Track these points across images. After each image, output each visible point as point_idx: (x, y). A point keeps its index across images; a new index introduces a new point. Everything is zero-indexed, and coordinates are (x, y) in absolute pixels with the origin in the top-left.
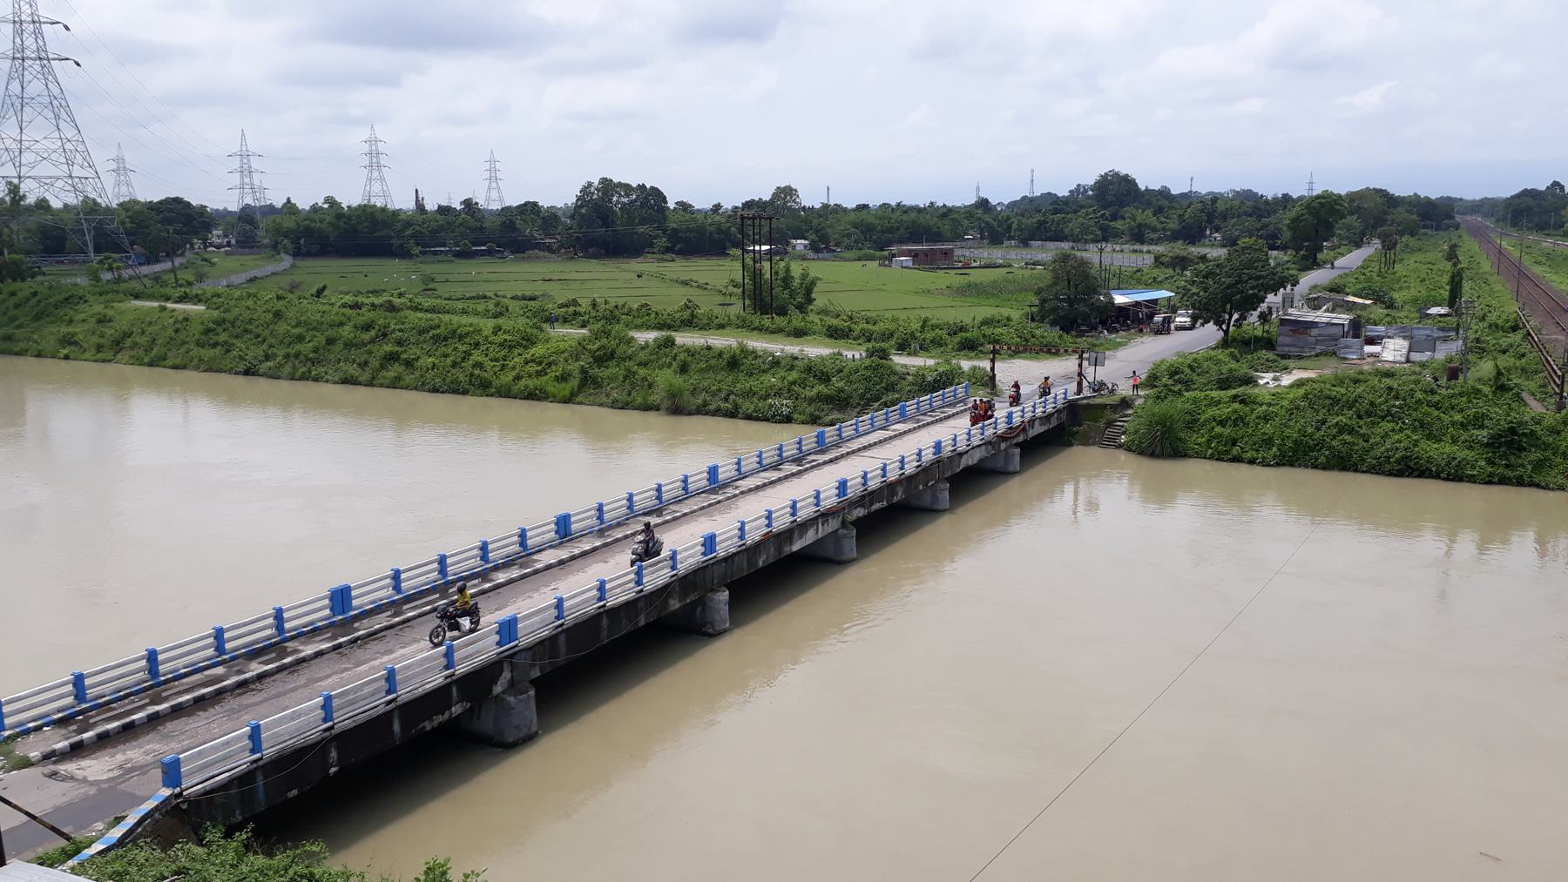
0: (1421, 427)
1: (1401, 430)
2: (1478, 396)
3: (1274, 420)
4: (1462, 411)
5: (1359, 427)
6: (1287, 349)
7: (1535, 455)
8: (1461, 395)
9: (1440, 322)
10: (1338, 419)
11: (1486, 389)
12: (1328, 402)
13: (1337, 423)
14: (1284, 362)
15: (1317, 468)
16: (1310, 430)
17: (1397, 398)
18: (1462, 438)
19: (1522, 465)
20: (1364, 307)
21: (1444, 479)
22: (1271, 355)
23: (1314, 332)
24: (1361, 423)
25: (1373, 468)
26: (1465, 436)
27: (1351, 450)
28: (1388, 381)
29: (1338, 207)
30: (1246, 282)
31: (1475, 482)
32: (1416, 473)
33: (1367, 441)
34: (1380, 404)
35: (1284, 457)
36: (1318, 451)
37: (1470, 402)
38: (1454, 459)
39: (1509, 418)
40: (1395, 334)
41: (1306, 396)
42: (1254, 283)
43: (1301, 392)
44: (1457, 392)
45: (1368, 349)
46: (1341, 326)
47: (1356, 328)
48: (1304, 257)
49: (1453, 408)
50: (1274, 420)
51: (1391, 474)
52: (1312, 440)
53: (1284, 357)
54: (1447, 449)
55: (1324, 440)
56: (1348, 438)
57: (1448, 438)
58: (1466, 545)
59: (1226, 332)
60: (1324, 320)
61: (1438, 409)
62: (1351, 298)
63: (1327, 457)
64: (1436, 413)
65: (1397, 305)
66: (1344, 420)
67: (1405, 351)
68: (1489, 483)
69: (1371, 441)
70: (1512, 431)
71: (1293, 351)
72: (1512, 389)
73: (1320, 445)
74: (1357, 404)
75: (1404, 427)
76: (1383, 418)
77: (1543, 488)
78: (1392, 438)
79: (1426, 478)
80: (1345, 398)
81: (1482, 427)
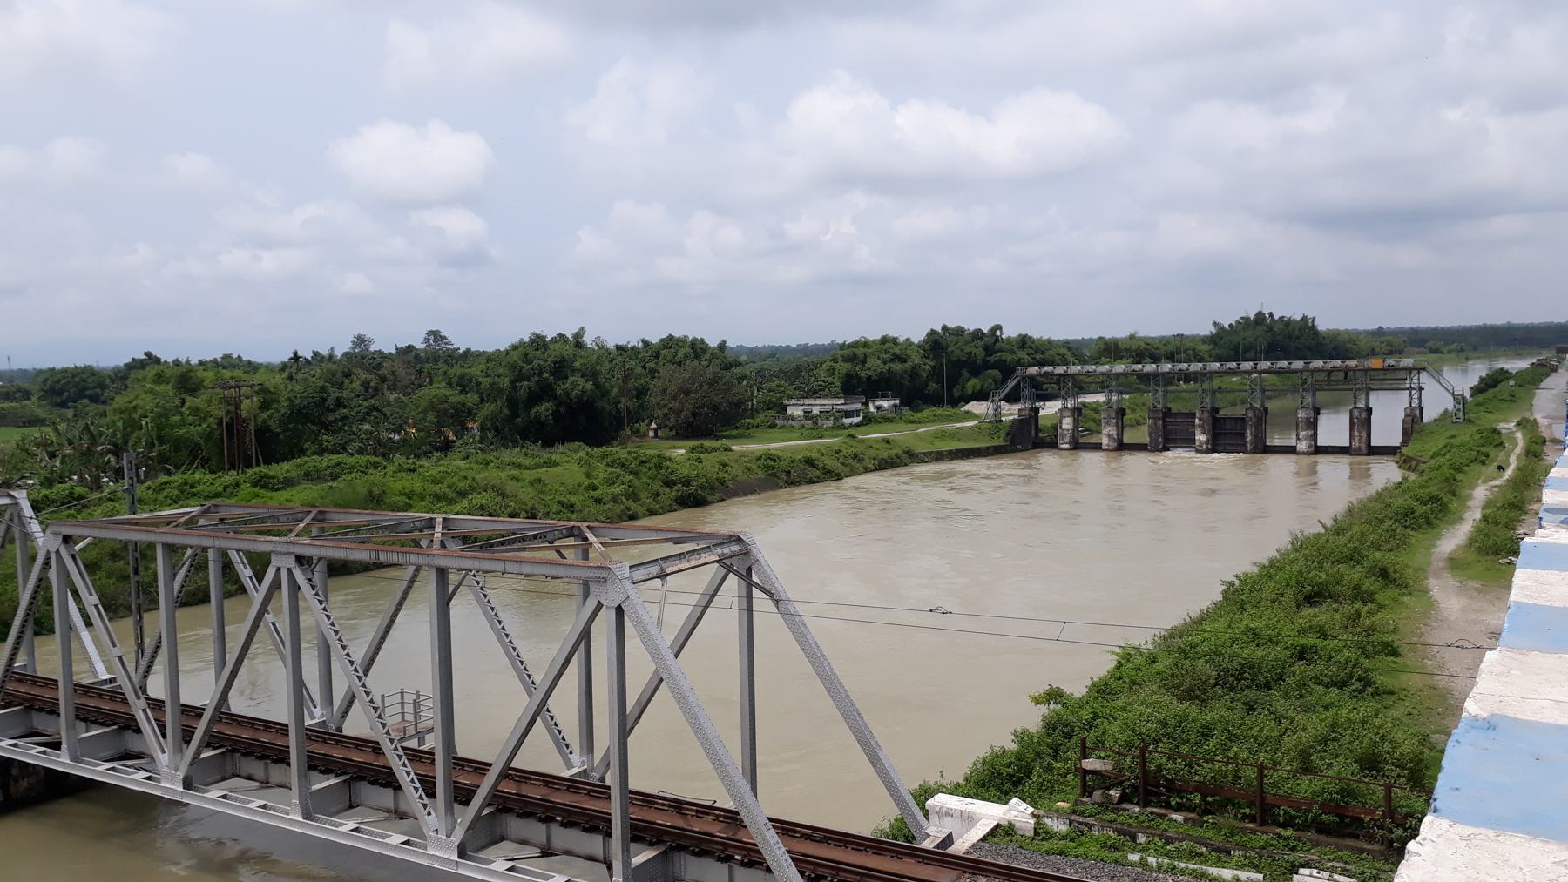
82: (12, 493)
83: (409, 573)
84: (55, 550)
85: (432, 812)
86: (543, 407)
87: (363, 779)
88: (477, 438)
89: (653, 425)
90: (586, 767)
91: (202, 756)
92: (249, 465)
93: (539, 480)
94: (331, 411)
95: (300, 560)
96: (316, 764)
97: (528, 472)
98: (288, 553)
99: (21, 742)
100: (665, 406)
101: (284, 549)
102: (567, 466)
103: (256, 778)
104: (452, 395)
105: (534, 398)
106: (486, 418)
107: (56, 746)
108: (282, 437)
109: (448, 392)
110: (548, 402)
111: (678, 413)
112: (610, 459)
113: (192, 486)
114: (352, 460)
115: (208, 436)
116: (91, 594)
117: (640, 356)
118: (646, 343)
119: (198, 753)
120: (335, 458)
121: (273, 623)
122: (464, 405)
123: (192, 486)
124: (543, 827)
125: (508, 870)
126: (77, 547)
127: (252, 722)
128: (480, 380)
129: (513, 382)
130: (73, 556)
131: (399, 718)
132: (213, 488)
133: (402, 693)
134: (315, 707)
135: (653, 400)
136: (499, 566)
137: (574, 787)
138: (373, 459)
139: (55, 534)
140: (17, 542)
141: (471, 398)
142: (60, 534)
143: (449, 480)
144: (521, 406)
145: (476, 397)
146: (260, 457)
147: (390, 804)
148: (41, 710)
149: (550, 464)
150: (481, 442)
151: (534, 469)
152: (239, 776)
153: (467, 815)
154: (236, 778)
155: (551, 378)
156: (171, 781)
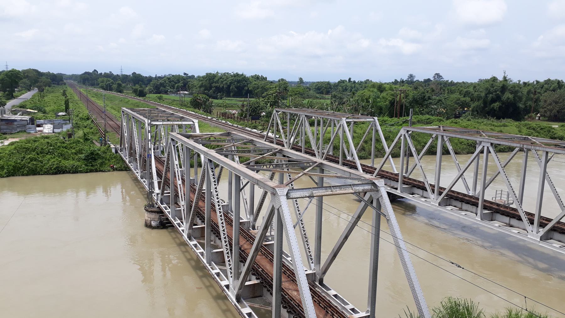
0: (61, 156)
1: (54, 157)
2: (79, 143)
4: (74, 148)
5: (38, 158)
6: (5, 131)
7: (100, 161)
8: (73, 143)
9: (63, 118)
10: (29, 156)
11: (81, 140)
13: (30, 157)
14: (4, 136)
15: (24, 176)
16: (19, 161)
17: (51, 146)
18: (76, 158)
19: (96, 165)
20: (35, 113)
21: (73, 173)
23: (15, 123)
24: (39, 156)
25: (46, 173)
26: (77, 157)
27: (36, 167)
28: (47, 140)
31: (82, 173)
33: (42, 163)
34: (45, 149)
35: (10, 173)
36: (23, 169)
37: (77, 145)
38: (74, 165)
40: (48, 123)
41: (15, 149)
43: (13, 147)
44: (72, 142)
45: (38, 129)
47: (32, 121)
48: (7, 95)
49: (71, 148)
50: (3, 159)
52: (21, 165)
53: (4, 134)
54: (72, 162)
55: (25, 164)
56: (35, 163)
58: (82, 194)
60: (20, 119)
61: (66, 149)
62: (29, 110)
64: (66, 150)
65: (47, 112)
66: (32, 156)
67: (52, 129)
68: (87, 172)
69: (44, 163)
70: (92, 153)
71: (8, 131)
72: (90, 140)
73: (24, 166)
74: (36, 150)
75: (55, 156)
76: (47, 154)
77: (104, 172)
78: (51, 161)
79: (65, 173)
80: (31, 148)
81: (82, 153)
82: (374, 117)
84: (404, 134)
86: (496, 104)
87: (498, 213)
89: (539, 115)
95: (492, 144)
97: (497, 128)
100: (545, 108)
101: (487, 141)
105: (493, 101)
106: (474, 107)
107: (396, 189)
109: (459, 96)
111: (551, 111)
112: (528, 126)
113: (385, 121)
115: (386, 105)
116: (413, 147)
117: (534, 87)
118: (538, 82)
119: (444, 196)
120: (428, 116)
121: (458, 164)
122: (465, 101)
123: (385, 121)
128: (473, 93)
129: (486, 94)
131: (499, 198)
133: (502, 191)
134: (470, 191)
135: (542, 104)
138: (440, 118)
139: (404, 130)
141: (468, 99)
142: (406, 130)
144: (488, 103)
145: (469, 99)
146: (406, 114)
147: (508, 222)
149: (505, 126)
151: (499, 127)
152: (451, 206)
154: (451, 206)
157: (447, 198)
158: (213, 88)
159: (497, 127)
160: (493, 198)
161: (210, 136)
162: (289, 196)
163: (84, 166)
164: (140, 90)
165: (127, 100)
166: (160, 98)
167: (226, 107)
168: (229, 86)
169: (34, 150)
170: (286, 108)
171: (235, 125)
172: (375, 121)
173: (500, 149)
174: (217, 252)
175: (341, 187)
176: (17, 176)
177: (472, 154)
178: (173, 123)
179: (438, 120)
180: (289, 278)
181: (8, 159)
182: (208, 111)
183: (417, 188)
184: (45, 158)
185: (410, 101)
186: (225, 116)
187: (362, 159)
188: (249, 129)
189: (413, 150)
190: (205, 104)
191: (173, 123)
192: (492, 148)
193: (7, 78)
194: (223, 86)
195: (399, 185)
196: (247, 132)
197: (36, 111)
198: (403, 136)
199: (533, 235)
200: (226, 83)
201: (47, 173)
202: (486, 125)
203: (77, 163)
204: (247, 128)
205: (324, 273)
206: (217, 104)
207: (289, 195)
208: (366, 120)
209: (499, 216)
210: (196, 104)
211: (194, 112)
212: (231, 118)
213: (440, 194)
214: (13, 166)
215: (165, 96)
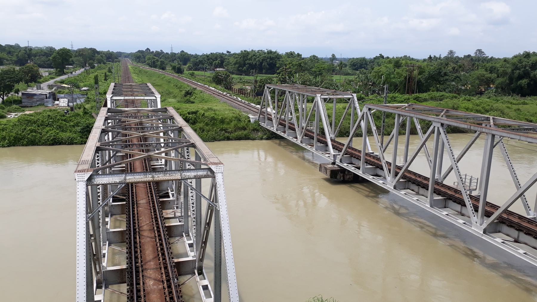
1: (53, 129)
3: (6, 130)
4: (73, 122)
5: (39, 130)
10: (30, 128)
11: (81, 114)
12: (26, 122)
13: (29, 129)
14: (23, 109)
17: (51, 119)
21: (68, 144)
22: (17, 106)
23: (35, 97)
24: (39, 128)
25: (44, 144)
26: (74, 130)
29: (69, 54)
30: (6, 79)
31: (77, 144)
32: (58, 144)
33: (41, 134)
34: (46, 121)
35: (11, 143)
37: (75, 118)
39: (86, 123)
41: (19, 121)
42: (9, 80)
45: (57, 102)
46: (45, 96)
48: (59, 71)
49: (70, 121)
50: (6, 130)
51: (50, 145)
52: (21, 136)
54: (68, 134)
56: (34, 134)
57: (68, 131)
59: (3, 99)
60: (39, 93)
63: (26, 141)
64: (64, 123)
66: (32, 128)
67: (67, 102)
71: (29, 105)
72: (89, 113)
73: (23, 138)
76: (47, 126)
78: (50, 133)
81: (79, 126)
82: (353, 94)
83: (476, 134)
85: (475, 216)
86: (524, 81)
87: (451, 199)
88: (494, 91)
90: (535, 217)
91: (400, 180)
92: (413, 93)
93: (519, 110)
94: (442, 77)
96: (437, 192)
97: (515, 106)
98: (438, 122)
99: (349, 165)
101: (438, 120)
102: (532, 105)
103: (415, 191)
104: (486, 74)
105: (520, 77)
106: (499, 84)
107: (359, 168)
108: (425, 84)
109: (485, 73)
110: (526, 79)
113: (395, 98)
114: (447, 95)
115: (401, 83)
119: (399, 179)
122: (490, 78)
123: (395, 98)
124: (517, 232)
125: (502, 242)
126: (372, 112)
127: (415, 174)
128: (499, 69)
129: (513, 70)
130: (371, 115)
132: (401, 99)
133: (466, 175)
136: (518, 137)
137: (530, 222)
138: (455, 95)
139: (366, 107)
140: (352, 108)
141: (494, 75)
142: (368, 107)
143: (483, 105)
144: (514, 80)
145: (496, 75)
147: (459, 210)
148: (355, 157)
149: (524, 104)
150: (495, 93)
152: (410, 189)
153: (488, 221)
154: (409, 190)
155: (530, 69)
156: (391, 186)
157: (406, 181)
158: (247, 65)
159: (515, 104)
160: (454, 183)
161: (137, 111)
162: (93, 182)
163: (79, 138)
164: (177, 67)
165: (163, 76)
166: (192, 75)
167: (244, 83)
168: (261, 63)
169: (35, 122)
170: (278, 84)
171: (243, 101)
172: (353, 98)
173: (453, 130)
174: (114, 231)
175: (166, 173)
176: (17, 146)
177: (83, 145)
178: (135, 98)
179: (452, 98)
180: (160, 264)
181: (11, 131)
182: (228, 87)
183: (380, 169)
184: (45, 130)
185: (426, 77)
186: (241, 92)
187: (358, 136)
188: (254, 105)
189: (374, 128)
190: (226, 81)
191: (135, 98)
192: (443, 128)
193: (58, 56)
194: (256, 63)
195: (361, 164)
196: (250, 108)
197: (69, 86)
198: (365, 114)
199: (477, 227)
200: (259, 60)
201: (45, 144)
202: (503, 103)
203: (74, 135)
204: (252, 104)
205: (201, 260)
206: (246, 81)
207: (93, 180)
208: (343, 97)
209: (451, 203)
210: (218, 80)
211: (215, 88)
212: (242, 94)
213: (396, 174)
214: (14, 137)
215: (196, 72)
